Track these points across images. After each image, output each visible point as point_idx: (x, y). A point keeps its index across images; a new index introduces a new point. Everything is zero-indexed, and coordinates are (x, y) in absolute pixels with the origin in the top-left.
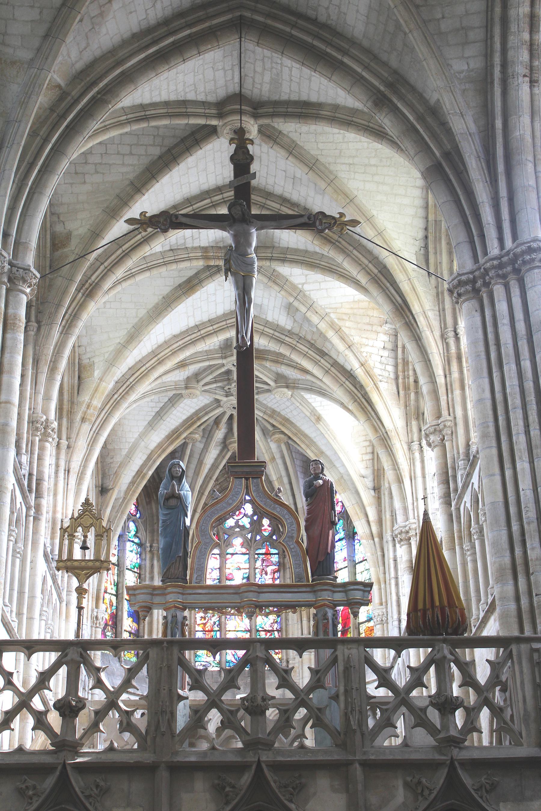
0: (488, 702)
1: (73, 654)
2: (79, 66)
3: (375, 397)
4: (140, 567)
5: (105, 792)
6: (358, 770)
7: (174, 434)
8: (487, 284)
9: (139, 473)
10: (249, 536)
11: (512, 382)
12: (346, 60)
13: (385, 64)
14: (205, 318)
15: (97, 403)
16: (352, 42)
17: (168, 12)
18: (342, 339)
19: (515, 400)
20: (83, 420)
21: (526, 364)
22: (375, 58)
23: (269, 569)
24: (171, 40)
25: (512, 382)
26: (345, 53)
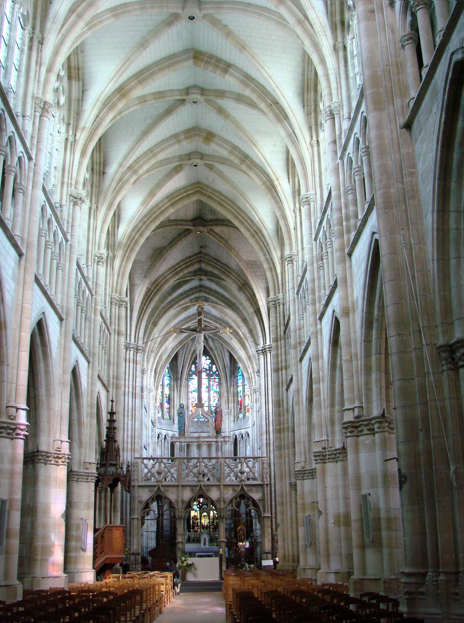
0: (251, 471)
1: (160, 460)
2: (153, 280)
3: (247, 344)
4: (170, 384)
5: (168, 491)
6: (222, 487)
8: (265, 352)
9: (169, 355)
10: (208, 372)
12: (231, 276)
13: (242, 278)
14: (191, 314)
15: (156, 346)
16: (232, 270)
17: (179, 261)
18: (237, 325)
20: (152, 351)
22: (239, 276)
23: (215, 384)
24: (180, 269)
26: (231, 274)
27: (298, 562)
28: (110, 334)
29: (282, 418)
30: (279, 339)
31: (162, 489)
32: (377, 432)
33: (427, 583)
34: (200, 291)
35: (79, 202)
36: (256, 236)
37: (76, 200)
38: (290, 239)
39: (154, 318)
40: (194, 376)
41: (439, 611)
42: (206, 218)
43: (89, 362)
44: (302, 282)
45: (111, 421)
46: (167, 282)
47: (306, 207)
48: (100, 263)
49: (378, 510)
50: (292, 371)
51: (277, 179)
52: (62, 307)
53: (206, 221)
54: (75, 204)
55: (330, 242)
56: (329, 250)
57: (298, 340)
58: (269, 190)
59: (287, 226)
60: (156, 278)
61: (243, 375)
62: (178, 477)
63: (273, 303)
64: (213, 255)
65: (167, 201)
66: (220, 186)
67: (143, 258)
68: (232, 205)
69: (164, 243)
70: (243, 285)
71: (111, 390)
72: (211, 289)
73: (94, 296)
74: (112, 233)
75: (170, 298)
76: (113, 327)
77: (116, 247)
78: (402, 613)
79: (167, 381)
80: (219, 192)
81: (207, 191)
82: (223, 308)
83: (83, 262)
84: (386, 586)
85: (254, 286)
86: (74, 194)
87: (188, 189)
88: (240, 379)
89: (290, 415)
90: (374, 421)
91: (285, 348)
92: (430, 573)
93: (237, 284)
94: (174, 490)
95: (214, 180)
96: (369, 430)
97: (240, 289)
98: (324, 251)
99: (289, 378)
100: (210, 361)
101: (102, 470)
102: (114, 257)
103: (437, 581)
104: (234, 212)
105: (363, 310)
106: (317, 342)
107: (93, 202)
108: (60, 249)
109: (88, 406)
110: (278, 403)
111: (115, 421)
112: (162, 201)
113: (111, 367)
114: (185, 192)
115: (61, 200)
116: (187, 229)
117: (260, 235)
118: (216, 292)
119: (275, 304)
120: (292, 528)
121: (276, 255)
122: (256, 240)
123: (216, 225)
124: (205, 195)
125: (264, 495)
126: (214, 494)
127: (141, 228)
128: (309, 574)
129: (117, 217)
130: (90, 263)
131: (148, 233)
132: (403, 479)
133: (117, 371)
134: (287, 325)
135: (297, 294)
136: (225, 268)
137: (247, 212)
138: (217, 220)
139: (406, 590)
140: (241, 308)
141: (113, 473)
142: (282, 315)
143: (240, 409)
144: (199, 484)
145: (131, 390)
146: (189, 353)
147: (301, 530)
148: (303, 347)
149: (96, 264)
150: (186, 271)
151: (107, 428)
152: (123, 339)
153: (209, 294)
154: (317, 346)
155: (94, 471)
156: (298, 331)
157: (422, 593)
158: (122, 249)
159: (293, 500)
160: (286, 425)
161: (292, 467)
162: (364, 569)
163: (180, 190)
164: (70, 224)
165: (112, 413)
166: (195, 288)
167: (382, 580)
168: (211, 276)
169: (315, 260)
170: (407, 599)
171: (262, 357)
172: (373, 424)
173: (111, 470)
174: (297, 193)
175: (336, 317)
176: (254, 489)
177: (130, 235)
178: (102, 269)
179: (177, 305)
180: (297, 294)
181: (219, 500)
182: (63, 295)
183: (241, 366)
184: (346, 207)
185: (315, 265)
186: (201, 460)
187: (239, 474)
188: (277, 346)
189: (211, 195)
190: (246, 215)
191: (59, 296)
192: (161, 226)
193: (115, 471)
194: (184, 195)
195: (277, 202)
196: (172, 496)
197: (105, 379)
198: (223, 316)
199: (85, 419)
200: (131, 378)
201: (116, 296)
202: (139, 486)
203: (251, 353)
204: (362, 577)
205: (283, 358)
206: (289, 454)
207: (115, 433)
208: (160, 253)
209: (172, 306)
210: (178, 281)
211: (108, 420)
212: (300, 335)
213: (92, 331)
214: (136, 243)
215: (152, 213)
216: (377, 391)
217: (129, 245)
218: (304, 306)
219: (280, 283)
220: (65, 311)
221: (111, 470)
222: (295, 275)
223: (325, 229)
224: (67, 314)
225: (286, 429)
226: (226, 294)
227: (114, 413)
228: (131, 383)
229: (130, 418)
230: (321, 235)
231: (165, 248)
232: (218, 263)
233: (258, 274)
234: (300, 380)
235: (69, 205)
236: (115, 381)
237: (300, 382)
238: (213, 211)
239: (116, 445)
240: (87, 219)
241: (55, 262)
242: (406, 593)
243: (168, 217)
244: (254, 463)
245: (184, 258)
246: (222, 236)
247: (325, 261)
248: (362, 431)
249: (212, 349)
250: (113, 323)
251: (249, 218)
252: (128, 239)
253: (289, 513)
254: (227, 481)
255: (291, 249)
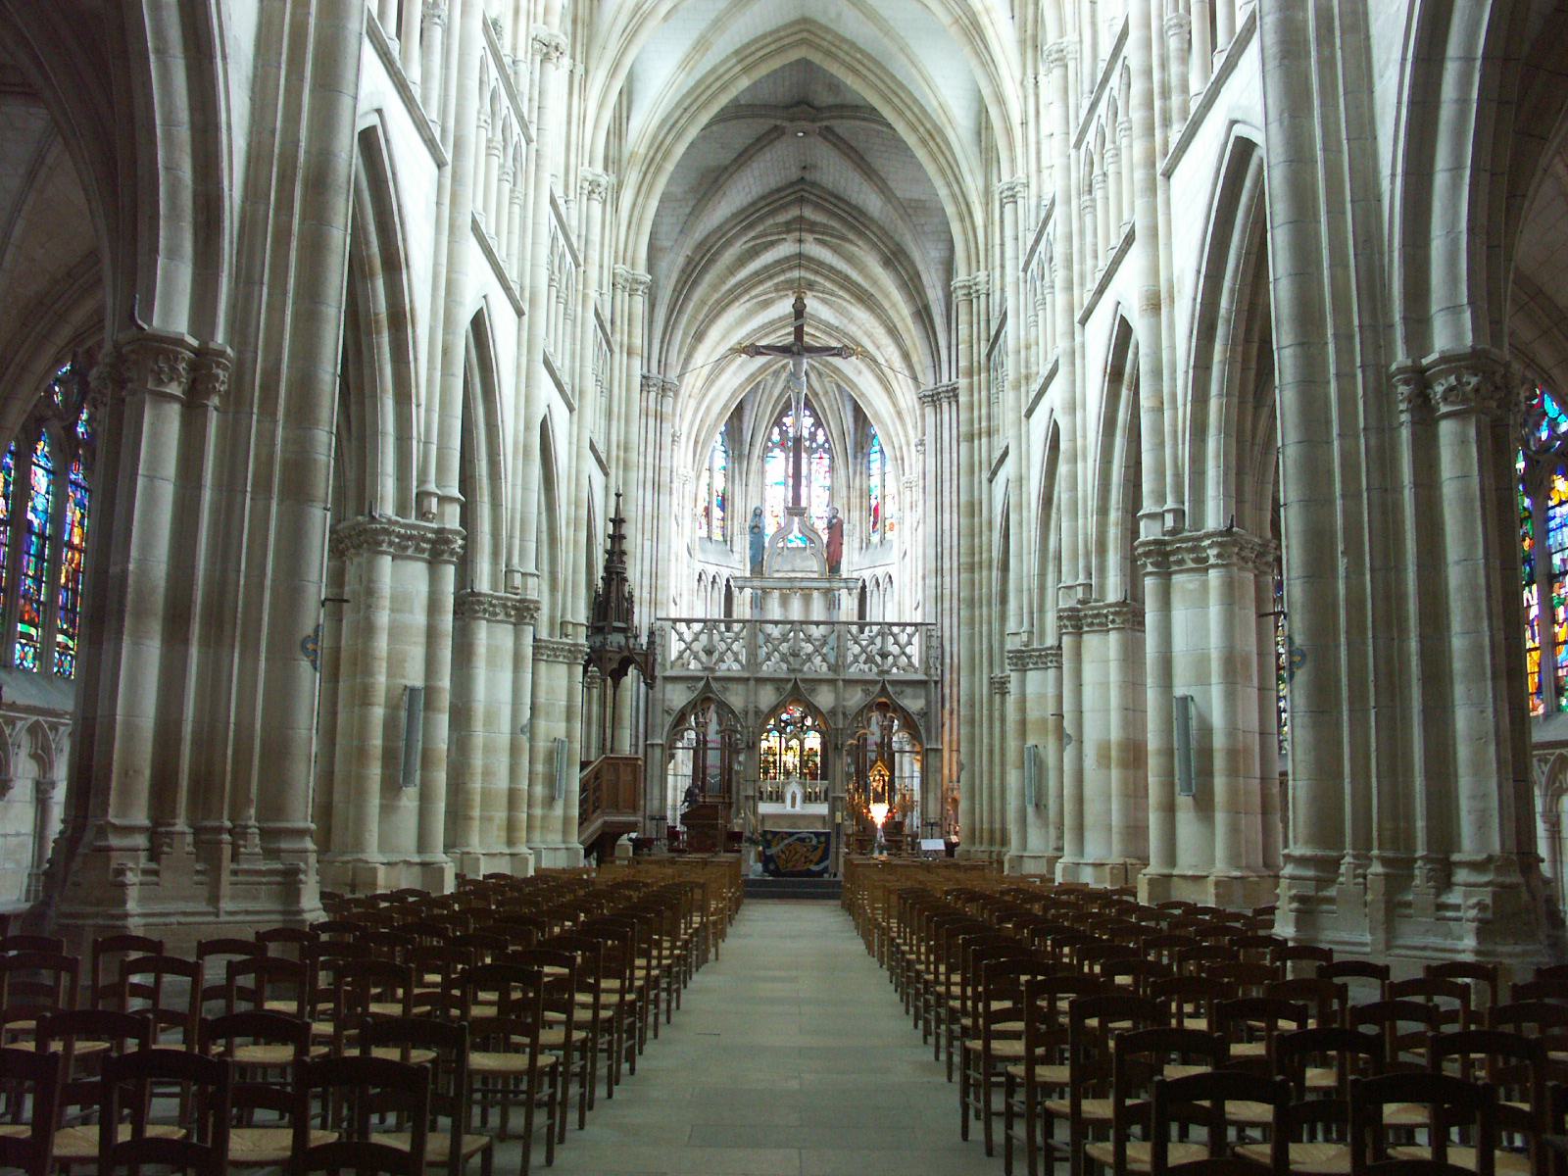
0: (904, 653)
5: (726, 689)
7: (753, 376)
9: (726, 406)
11: (946, 464)
15: (699, 384)
16: (871, 219)
18: (873, 342)
19: (946, 476)
21: (955, 455)
25: (946, 464)
26: (868, 228)
27: (1004, 842)
28: (611, 350)
29: (976, 540)
30: (975, 369)
31: (714, 685)
32: (1213, 566)
33: (1341, 879)
34: (800, 266)
35: (554, 55)
36: (931, 143)
37: (547, 51)
38: (1011, 147)
39: (697, 324)
40: (777, 452)
41: (1368, 938)
42: (817, 103)
43: (571, 410)
44: (1037, 241)
45: (617, 538)
46: (729, 243)
47: (1057, 72)
48: (595, 196)
49: (1206, 730)
50: (1007, 436)
51: (987, 11)
52: (522, 288)
53: (818, 109)
54: (546, 58)
55: (1113, 152)
56: (1111, 170)
57: (1023, 371)
58: (966, 33)
59: (1006, 118)
60: (704, 234)
61: (882, 451)
62: (748, 661)
63: (965, 291)
64: (830, 186)
65: (734, 60)
66: (853, 26)
67: (678, 190)
68: (878, 72)
69: (726, 157)
70: (893, 253)
71: (613, 472)
72: (820, 263)
73: (582, 269)
74: (618, 130)
75: (733, 281)
76: (618, 336)
77: (624, 163)
78: (1286, 941)
79: (720, 460)
80: (853, 45)
81: (824, 39)
82: (845, 304)
83: (559, 193)
84: (1221, 890)
85: (916, 255)
86: (543, 36)
87: (782, 34)
88: (875, 457)
89: (996, 536)
90: (1208, 542)
91: (989, 390)
92: (1347, 859)
93: (879, 250)
94: (740, 688)
95: (839, 15)
96: (1197, 560)
97: (887, 263)
98: (1097, 170)
99: (997, 454)
100: (812, 420)
101: (598, 639)
102: (620, 185)
103: (1365, 877)
104: (883, 87)
105: (1195, 299)
106: (1073, 373)
107: (578, 57)
108: (514, 159)
109: (569, 504)
110: (972, 509)
111: (623, 537)
112: (723, 62)
113: (614, 423)
114: (774, 42)
115: (514, 49)
116: (776, 127)
117: (938, 140)
118: (831, 268)
119: (970, 294)
120: (991, 773)
121: (973, 185)
122: (931, 153)
123: (842, 118)
124: (817, 48)
125: (928, 703)
126: (824, 699)
127: (677, 122)
128: (1031, 868)
129: (627, 96)
130: (571, 196)
131: (692, 133)
132: (1297, 659)
133: (627, 433)
134: (994, 342)
135: (1025, 270)
136: (854, 213)
137: (911, 88)
138: (843, 107)
139: (1293, 892)
140: (887, 305)
141: (620, 647)
142: (983, 317)
143: (875, 524)
144: (793, 676)
145: (650, 474)
146: (768, 401)
147: (1013, 778)
148: (1035, 387)
149: (585, 198)
150: (770, 221)
151: (607, 552)
152: (637, 362)
153: (817, 273)
154: (1073, 382)
155: (582, 640)
156: (1023, 353)
157: (1330, 900)
158: (637, 168)
159: (997, 714)
160: (984, 556)
161: (996, 645)
162: (1170, 856)
163: (764, 36)
164: (536, 104)
165: (618, 521)
166: (787, 259)
167: (1212, 879)
168: (823, 234)
169: (1074, 193)
170: (1297, 910)
171: (929, 411)
172: (1204, 549)
173: (617, 639)
174: (1029, 43)
175: (1123, 318)
176: (909, 691)
177: (655, 137)
178: (596, 207)
179: (747, 297)
180: (1025, 270)
181: (833, 712)
182: (522, 259)
183: (880, 435)
184: (1164, 65)
185: (1074, 202)
186: (798, 627)
187: (878, 659)
188: (971, 385)
189: (833, 49)
190: (910, 94)
191: (515, 260)
192: (722, 118)
193: (623, 642)
194: (773, 47)
195: (984, 64)
196: (736, 699)
197: (601, 448)
198: (846, 321)
199: (564, 531)
200: (650, 450)
201: (621, 269)
202: (666, 679)
203: (902, 404)
204: (1166, 871)
205: (984, 411)
206: (990, 616)
207: (623, 562)
208: (716, 180)
209: (737, 298)
210: (752, 243)
211: (609, 536)
212: (1027, 362)
213: (578, 343)
214: (664, 158)
215: (703, 87)
216: (1218, 477)
217: (653, 159)
218: (1039, 297)
219: (981, 247)
220: (527, 294)
221: (617, 639)
222: (1021, 228)
223: (1103, 120)
224: (532, 302)
225: (985, 564)
226: (855, 275)
227: (622, 521)
228: (650, 460)
229: (647, 535)
230: (1090, 136)
231: (726, 168)
232: (840, 204)
233: (1286, 62)
234: (1023, 459)
235: (532, 63)
236: (622, 454)
237: (1024, 462)
238: (835, 86)
239: (627, 589)
240: (566, 96)
241: (507, 187)
242: (1293, 899)
243: (736, 99)
244: (910, 636)
245: (767, 190)
246: (854, 144)
247: (1098, 194)
248: (1181, 562)
249: (816, 395)
250: (618, 329)
251: (915, 101)
252: (650, 147)
253: (985, 741)
254: (853, 671)
255: (1013, 173)
